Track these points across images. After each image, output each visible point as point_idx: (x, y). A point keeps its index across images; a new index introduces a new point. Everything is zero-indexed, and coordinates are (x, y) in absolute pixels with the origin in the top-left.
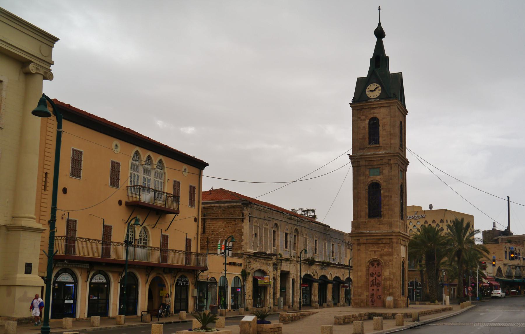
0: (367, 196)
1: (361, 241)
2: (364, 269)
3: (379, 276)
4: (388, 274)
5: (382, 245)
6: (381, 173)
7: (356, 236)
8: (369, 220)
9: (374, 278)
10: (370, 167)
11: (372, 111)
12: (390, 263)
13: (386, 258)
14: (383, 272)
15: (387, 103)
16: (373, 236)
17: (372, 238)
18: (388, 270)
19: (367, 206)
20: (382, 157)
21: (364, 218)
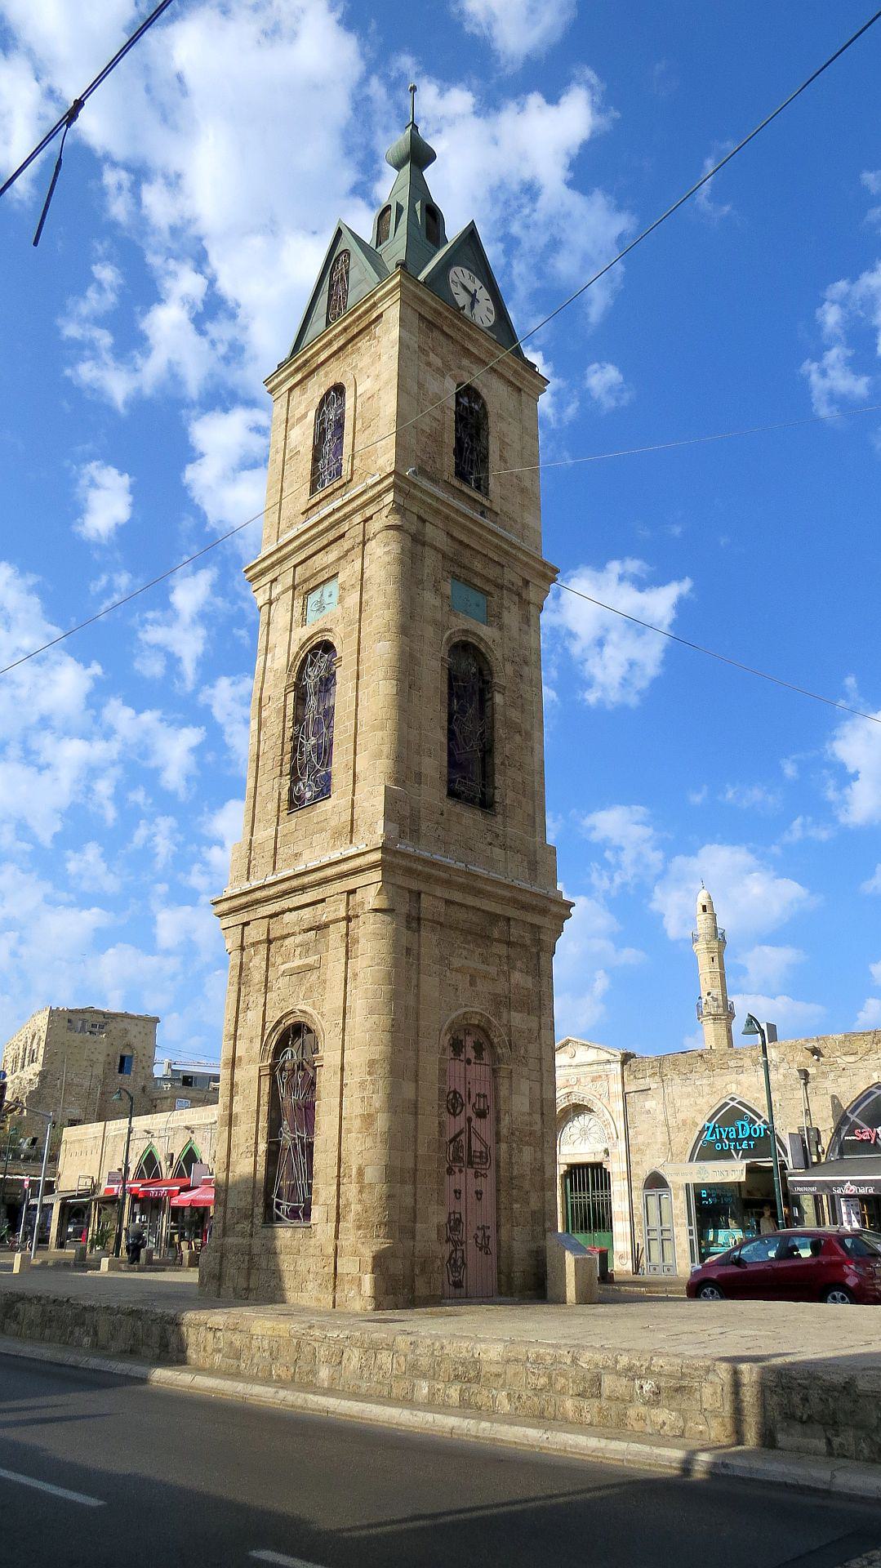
0: (445, 689)
1: (425, 902)
2: (430, 1065)
3: (481, 1114)
4: (526, 1109)
5: (502, 950)
6: (493, 617)
7: (409, 872)
8: (448, 804)
9: (460, 1122)
10: (457, 571)
11: (465, 362)
12: (531, 1047)
13: (517, 1019)
14: (504, 1092)
15: (515, 371)
16: (478, 893)
17: (471, 901)
18: (525, 1086)
19: (445, 741)
20: (507, 553)
21: (433, 794)
